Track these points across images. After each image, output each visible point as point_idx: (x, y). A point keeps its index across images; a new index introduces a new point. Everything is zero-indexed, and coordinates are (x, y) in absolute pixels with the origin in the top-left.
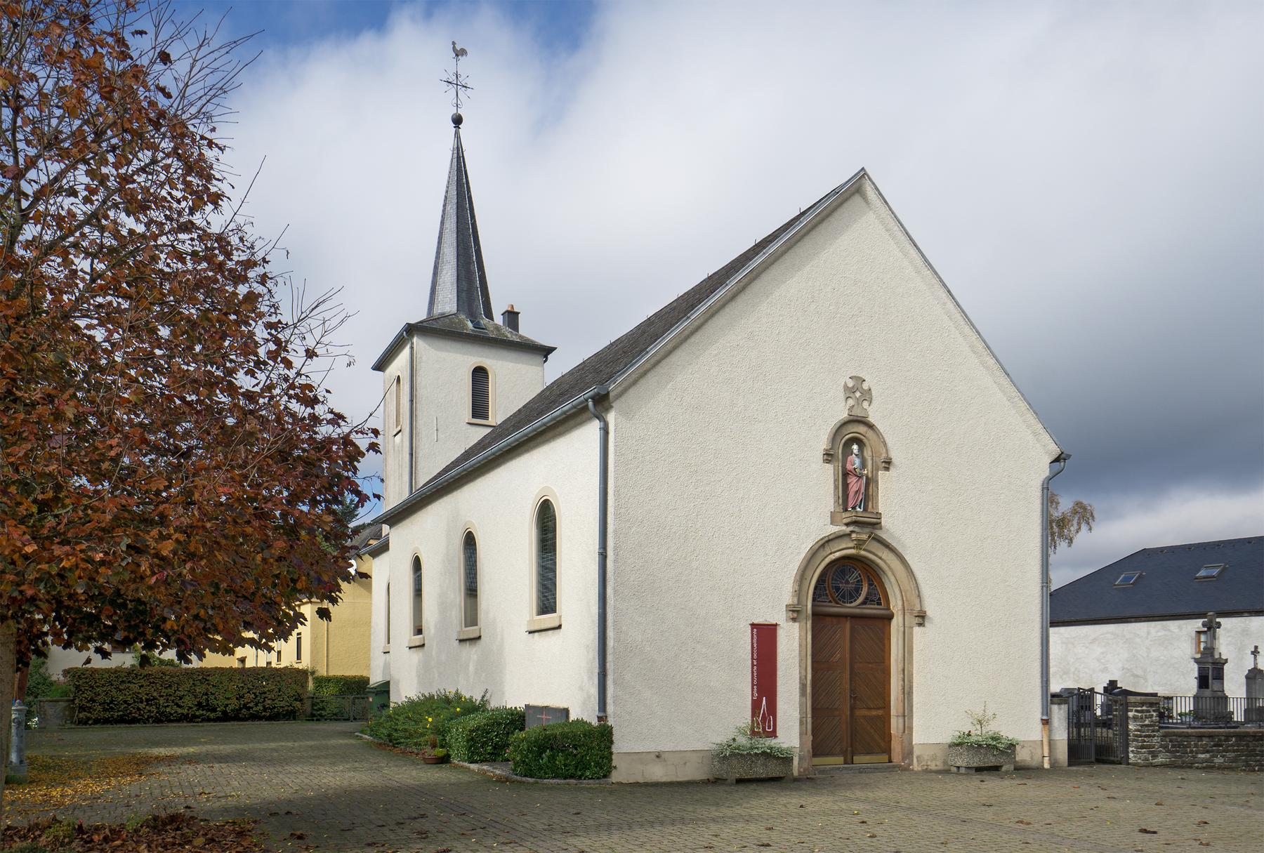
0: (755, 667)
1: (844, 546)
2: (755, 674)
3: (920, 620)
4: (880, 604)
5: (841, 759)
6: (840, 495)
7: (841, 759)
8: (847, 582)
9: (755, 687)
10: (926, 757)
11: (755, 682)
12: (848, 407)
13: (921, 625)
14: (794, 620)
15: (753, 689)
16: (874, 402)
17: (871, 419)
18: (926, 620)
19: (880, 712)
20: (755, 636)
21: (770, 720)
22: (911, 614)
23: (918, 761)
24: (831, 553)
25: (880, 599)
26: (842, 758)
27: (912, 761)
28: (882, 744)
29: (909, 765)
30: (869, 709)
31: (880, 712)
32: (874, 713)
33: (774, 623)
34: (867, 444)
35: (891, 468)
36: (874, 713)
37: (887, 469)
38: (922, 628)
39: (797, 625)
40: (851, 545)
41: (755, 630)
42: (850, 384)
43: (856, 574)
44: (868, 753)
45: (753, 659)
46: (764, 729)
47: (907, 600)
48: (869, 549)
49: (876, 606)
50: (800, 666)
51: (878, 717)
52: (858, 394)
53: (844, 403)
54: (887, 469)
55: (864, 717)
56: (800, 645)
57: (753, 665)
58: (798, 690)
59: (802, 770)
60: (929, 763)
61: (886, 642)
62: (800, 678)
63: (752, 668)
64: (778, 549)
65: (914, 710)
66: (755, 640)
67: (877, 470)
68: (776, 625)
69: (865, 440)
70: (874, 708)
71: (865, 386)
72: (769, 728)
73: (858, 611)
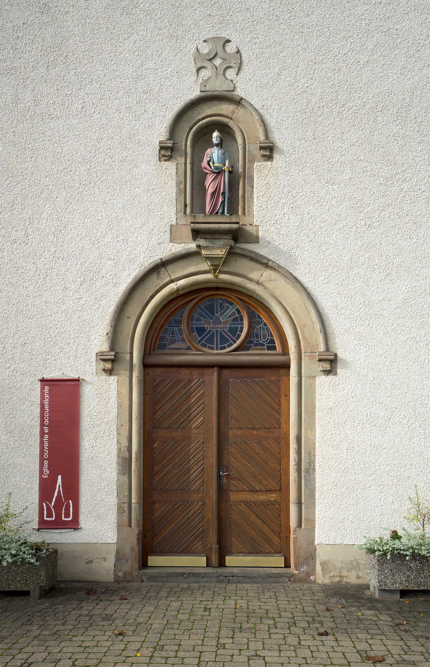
0: (46, 437)
1: (192, 269)
2: (46, 445)
3: (327, 366)
4: (274, 348)
5: (202, 560)
6: (188, 201)
7: (202, 560)
8: (218, 321)
9: (46, 463)
10: (339, 565)
11: (46, 455)
12: (200, 81)
13: (328, 372)
14: (110, 372)
15: (41, 465)
16: (245, 67)
17: (240, 92)
18: (339, 366)
19: (273, 497)
20: (47, 396)
21: (68, 506)
22: (311, 357)
23: (323, 569)
24: (172, 281)
25: (272, 341)
26: (204, 559)
27: (314, 568)
28: (276, 540)
29: (308, 575)
30: (253, 491)
31: (273, 497)
32: (262, 497)
33: (76, 377)
34: (235, 128)
35: (276, 156)
36: (262, 497)
37: (269, 158)
38: (330, 377)
39: (113, 379)
40: (205, 266)
41: (47, 388)
42: (205, 49)
43: (231, 310)
44: (250, 553)
45: (42, 424)
46: (59, 516)
47: (305, 339)
48: (242, 272)
49: (266, 352)
50: (118, 434)
51: (269, 503)
52: (218, 62)
53: (194, 78)
54: (269, 158)
55: (247, 503)
56: (120, 406)
57: (42, 433)
58: (114, 465)
59: (121, 574)
60: (345, 573)
61: (283, 400)
62: (119, 450)
63: (42, 437)
64: (84, 281)
65: (317, 495)
66: (46, 402)
67: (252, 161)
68: (77, 382)
69: (231, 124)
70: (261, 491)
71: (231, 48)
72: (67, 515)
73: (229, 359)
